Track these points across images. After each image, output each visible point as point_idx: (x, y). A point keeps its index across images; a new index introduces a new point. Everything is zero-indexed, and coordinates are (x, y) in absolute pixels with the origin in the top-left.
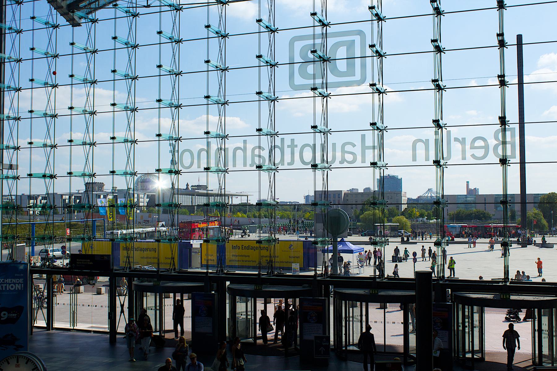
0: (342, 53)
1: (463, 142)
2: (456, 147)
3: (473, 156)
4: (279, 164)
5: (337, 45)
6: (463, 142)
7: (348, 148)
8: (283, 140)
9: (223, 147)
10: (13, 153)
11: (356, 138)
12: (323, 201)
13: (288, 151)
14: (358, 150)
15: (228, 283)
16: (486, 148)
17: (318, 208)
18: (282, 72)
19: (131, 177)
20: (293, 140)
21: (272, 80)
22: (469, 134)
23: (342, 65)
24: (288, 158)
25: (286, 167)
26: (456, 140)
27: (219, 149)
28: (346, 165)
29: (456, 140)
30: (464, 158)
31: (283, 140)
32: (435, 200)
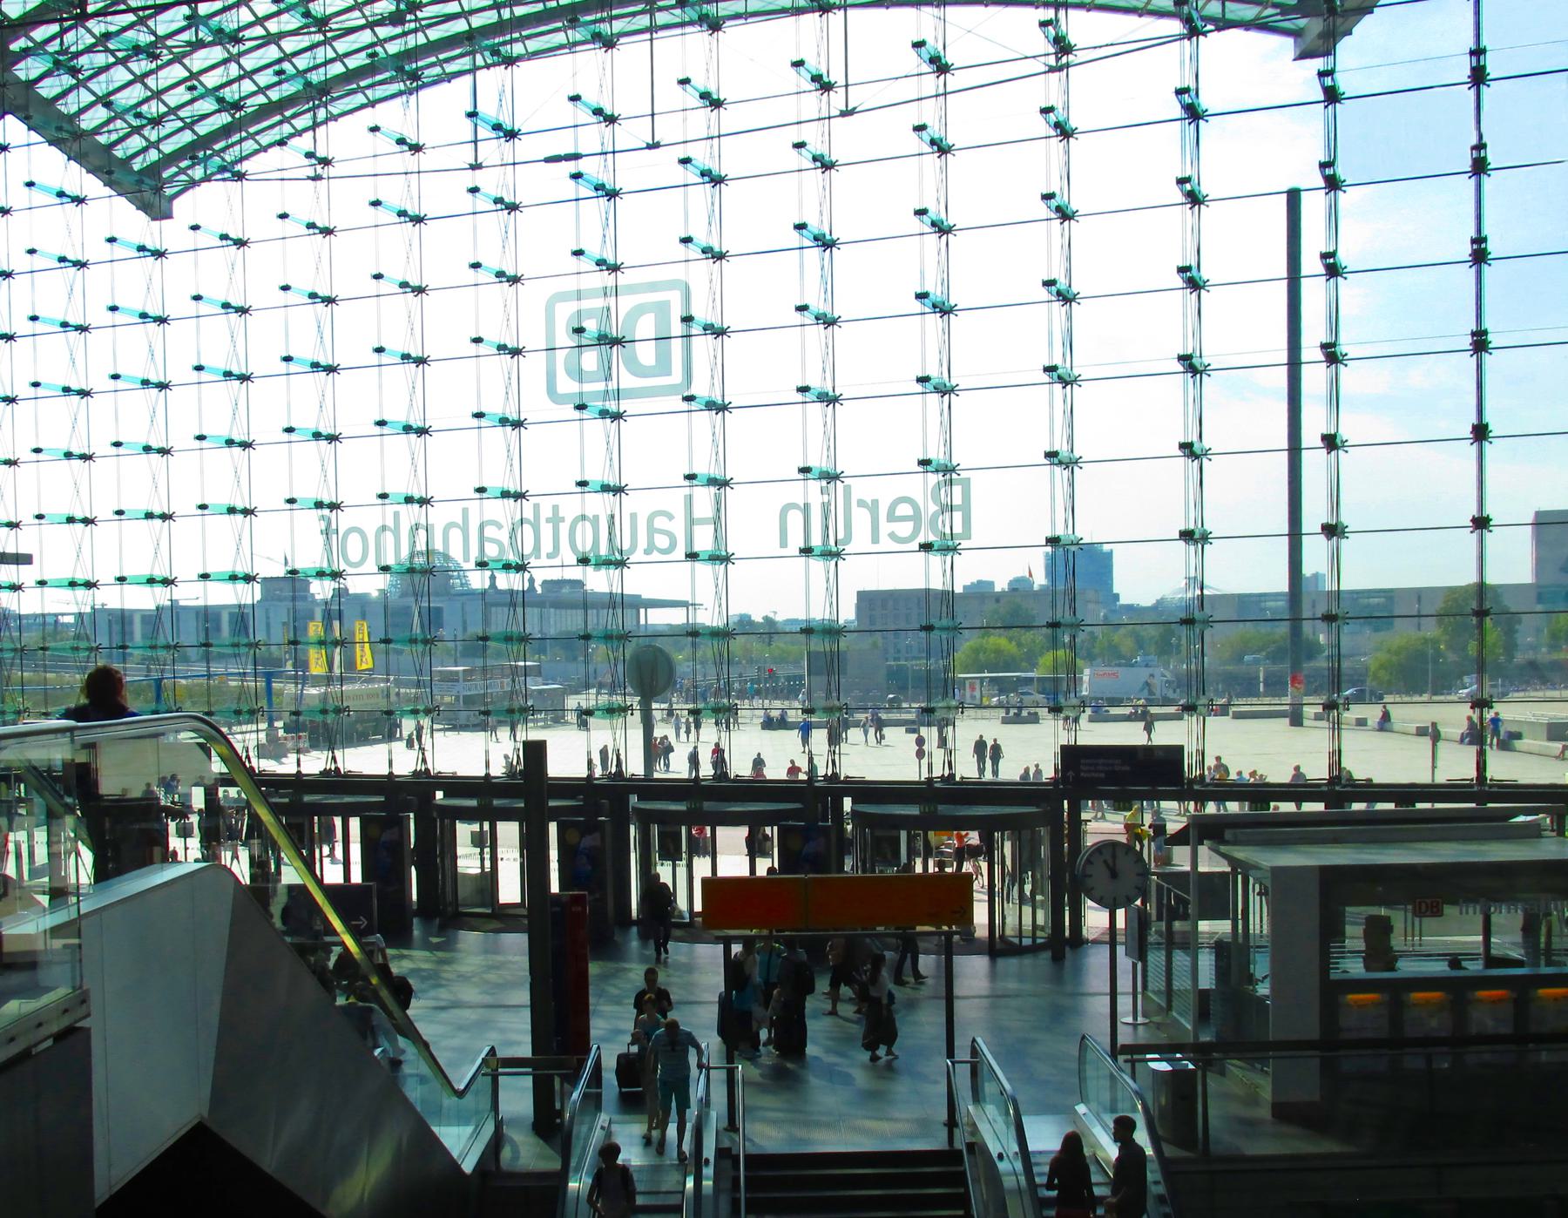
0: (646, 327)
1: (873, 507)
2: (861, 518)
3: (892, 536)
4: (530, 556)
6: (873, 507)
7: (660, 522)
8: (536, 507)
9: (423, 522)
10: (162, 528)
11: (674, 501)
12: (945, 622)
13: (546, 531)
14: (678, 527)
15: (439, 795)
17: (935, 635)
18: (533, 365)
19: (423, 579)
20: (555, 508)
21: (515, 384)
22: (885, 492)
23: (646, 353)
24: (546, 547)
25: (544, 561)
26: (861, 503)
27: (414, 528)
28: (656, 556)
29: (861, 503)
30: (875, 540)
31: (536, 507)
32: (804, 626)
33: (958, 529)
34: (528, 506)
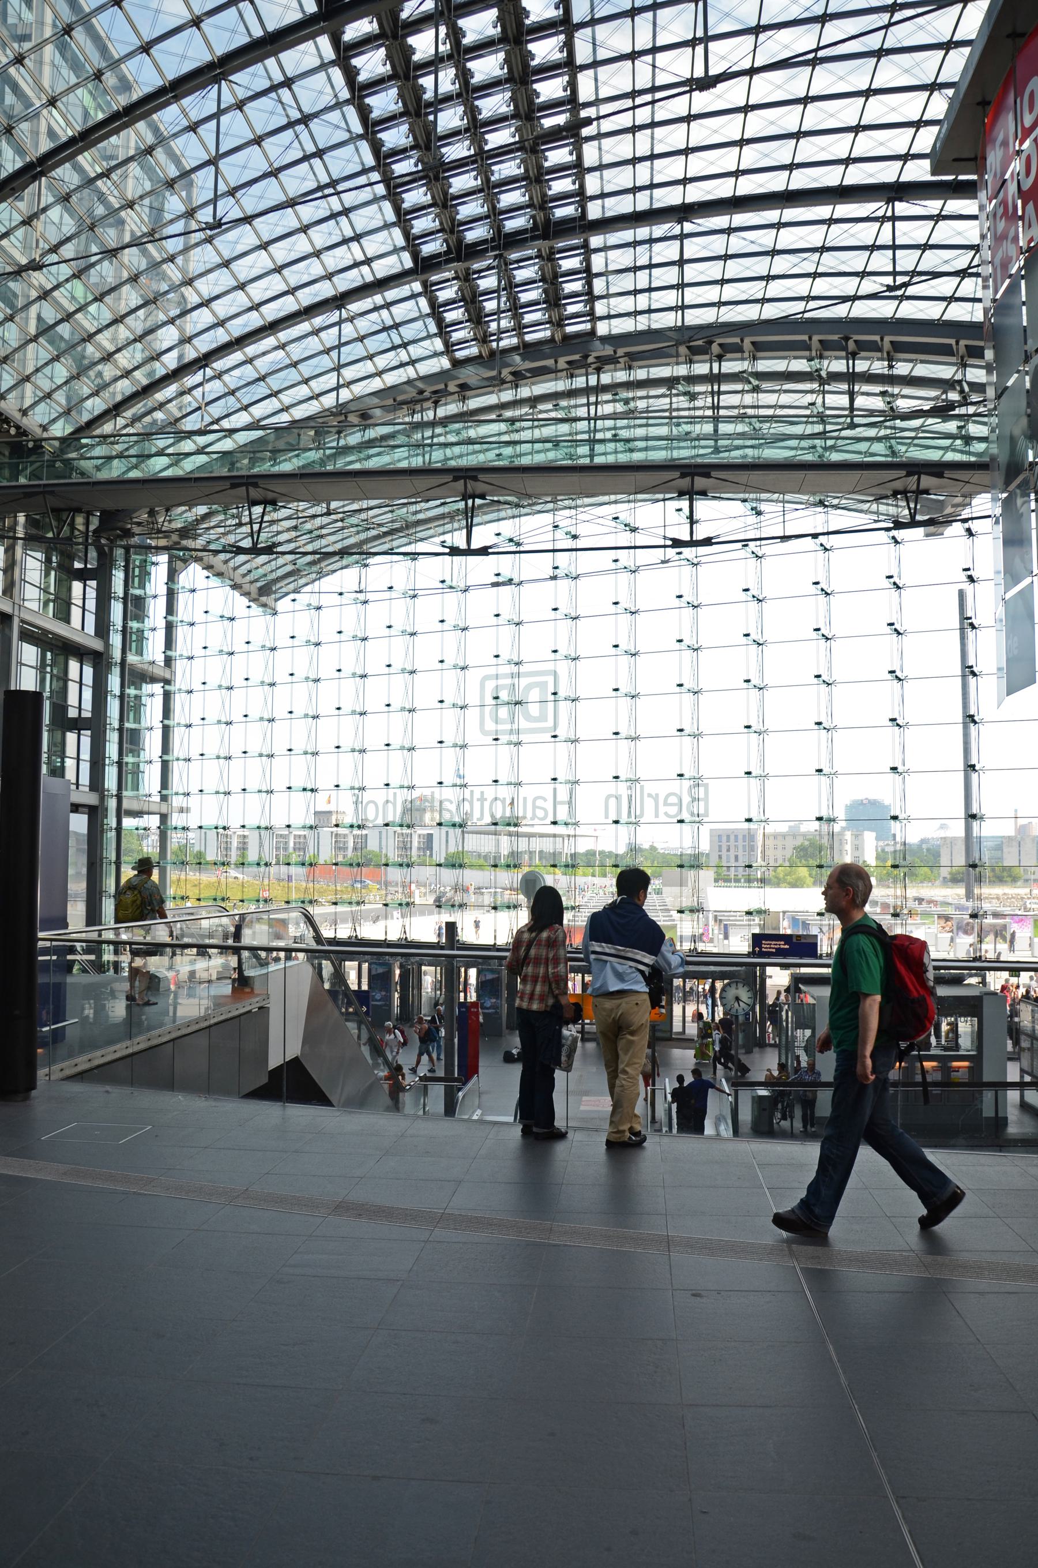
1: (656, 798)
2: (649, 804)
3: (666, 814)
5: (529, 687)
6: (656, 798)
7: (539, 803)
8: (472, 792)
18: (472, 714)
20: (482, 793)
23: (534, 709)
26: (649, 795)
29: (649, 795)
30: (657, 816)
31: (472, 792)
33: (701, 812)
34: (467, 791)
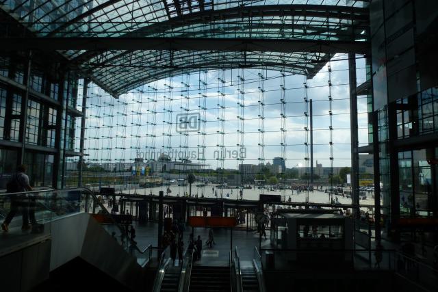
2: (228, 154)
5: (192, 117)
13: (174, 154)
14: (197, 154)
16: (237, 154)
22: (232, 149)
23: (193, 125)
